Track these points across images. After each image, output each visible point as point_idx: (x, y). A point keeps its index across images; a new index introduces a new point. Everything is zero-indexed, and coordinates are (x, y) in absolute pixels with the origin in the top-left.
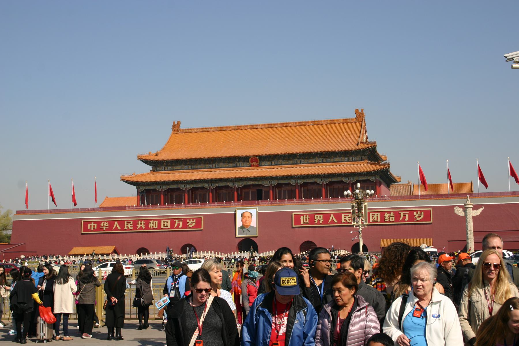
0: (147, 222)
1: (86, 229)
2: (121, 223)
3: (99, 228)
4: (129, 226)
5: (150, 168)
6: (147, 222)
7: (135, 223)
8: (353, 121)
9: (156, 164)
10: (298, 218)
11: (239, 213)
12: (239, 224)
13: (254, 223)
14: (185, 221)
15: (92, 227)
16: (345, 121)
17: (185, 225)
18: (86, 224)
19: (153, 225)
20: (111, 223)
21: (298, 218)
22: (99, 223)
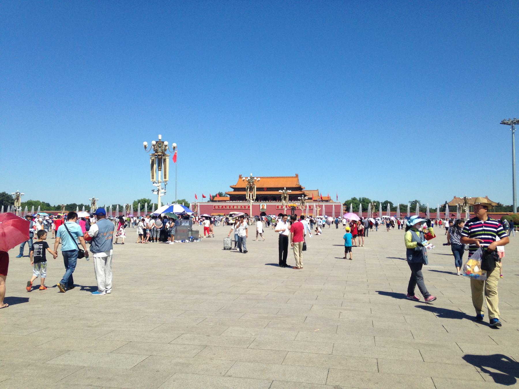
0: (233, 206)
1: (215, 207)
2: (226, 206)
3: (219, 208)
4: (228, 207)
5: (233, 190)
6: (233, 206)
7: (230, 206)
8: (295, 177)
9: (236, 189)
10: (278, 207)
11: (261, 205)
12: (261, 208)
13: (265, 208)
14: (245, 207)
15: (217, 207)
16: (292, 177)
17: (245, 207)
18: (215, 206)
19: (235, 207)
20: (223, 206)
21: (278, 207)
22: (219, 206)
